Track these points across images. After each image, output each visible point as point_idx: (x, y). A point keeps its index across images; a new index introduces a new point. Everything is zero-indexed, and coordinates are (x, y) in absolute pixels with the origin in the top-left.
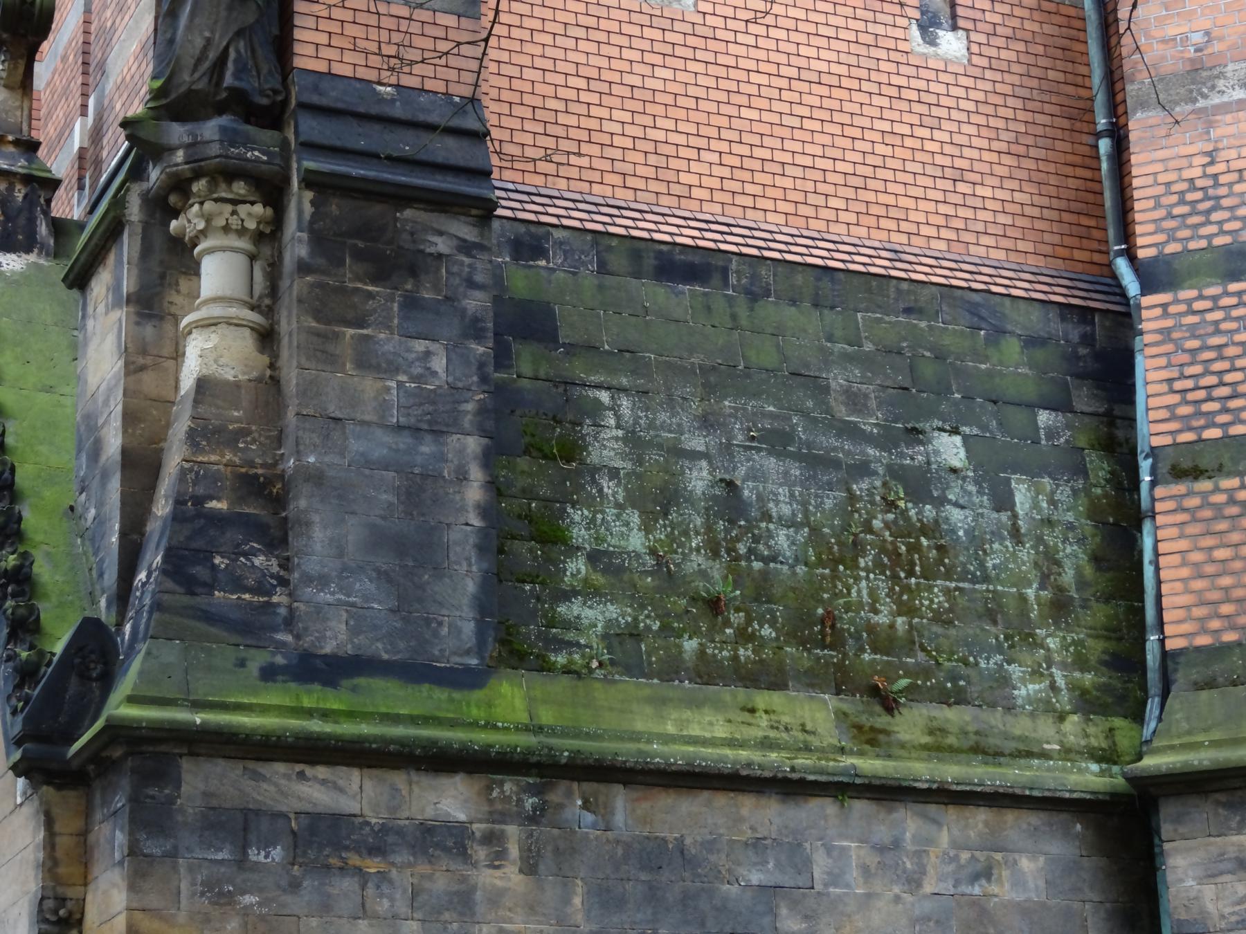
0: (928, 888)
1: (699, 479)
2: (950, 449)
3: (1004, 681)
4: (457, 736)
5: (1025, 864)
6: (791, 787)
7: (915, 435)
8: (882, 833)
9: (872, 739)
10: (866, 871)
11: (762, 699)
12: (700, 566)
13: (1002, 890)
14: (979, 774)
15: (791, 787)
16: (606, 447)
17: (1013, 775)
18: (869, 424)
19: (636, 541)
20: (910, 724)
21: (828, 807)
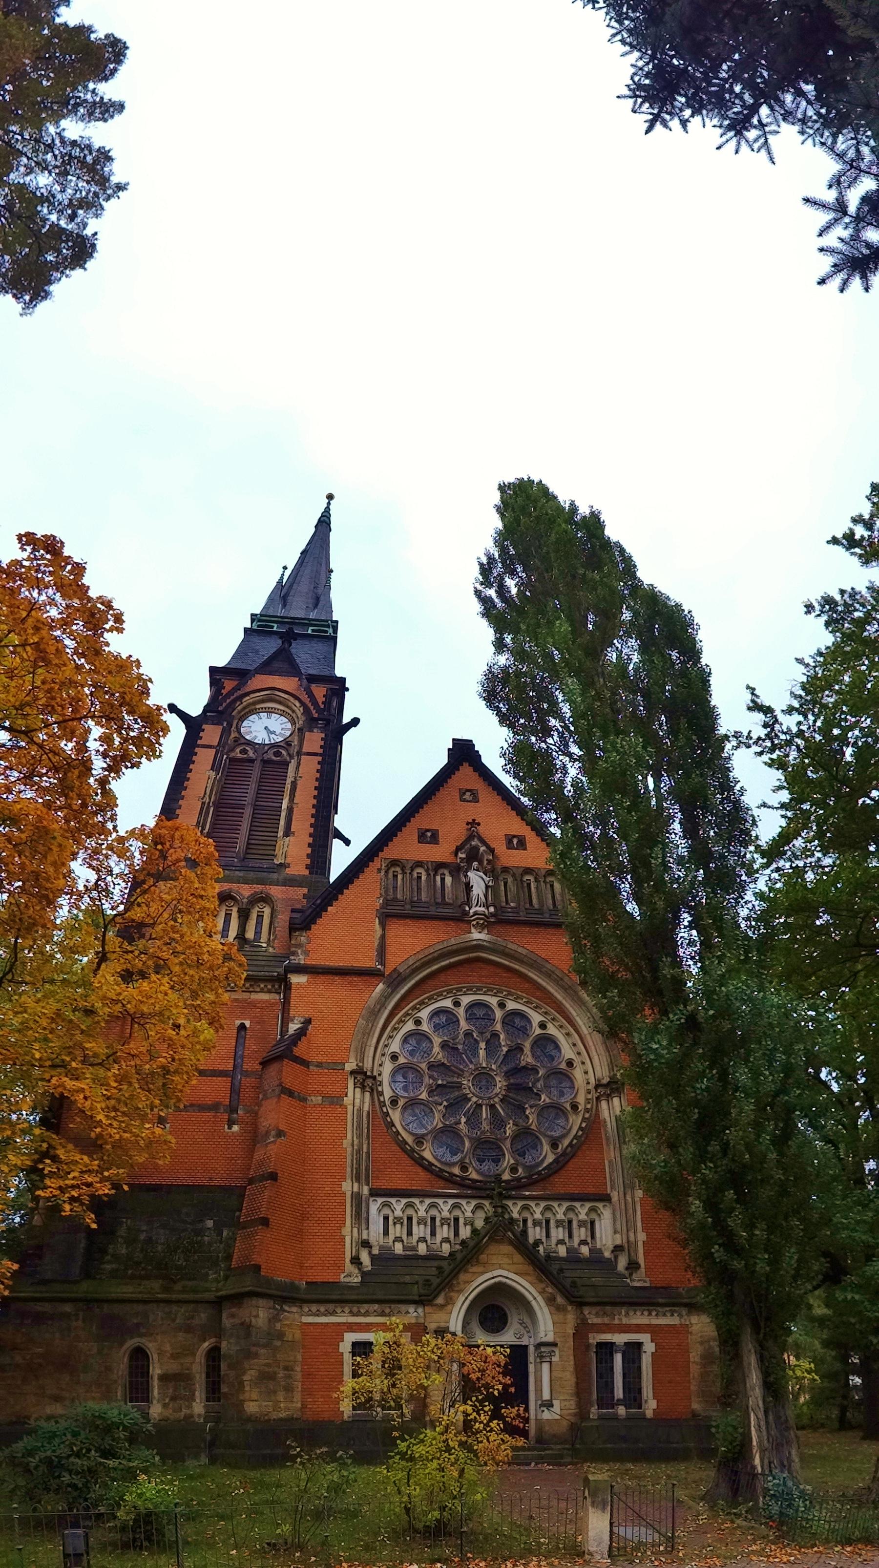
0: (178, 1321)
1: (142, 1237)
2: (210, 1223)
3: (207, 1274)
4: (73, 1295)
5: (202, 1315)
6: (145, 1302)
7: (201, 1221)
8: (167, 1310)
9: (166, 1289)
10: (162, 1319)
11: (144, 1282)
12: (138, 1256)
13: (196, 1322)
14: (191, 1296)
15: (145, 1302)
16: (122, 1231)
17: (199, 1296)
18: (189, 1220)
19: (124, 1251)
20: (178, 1287)
21: (155, 1305)
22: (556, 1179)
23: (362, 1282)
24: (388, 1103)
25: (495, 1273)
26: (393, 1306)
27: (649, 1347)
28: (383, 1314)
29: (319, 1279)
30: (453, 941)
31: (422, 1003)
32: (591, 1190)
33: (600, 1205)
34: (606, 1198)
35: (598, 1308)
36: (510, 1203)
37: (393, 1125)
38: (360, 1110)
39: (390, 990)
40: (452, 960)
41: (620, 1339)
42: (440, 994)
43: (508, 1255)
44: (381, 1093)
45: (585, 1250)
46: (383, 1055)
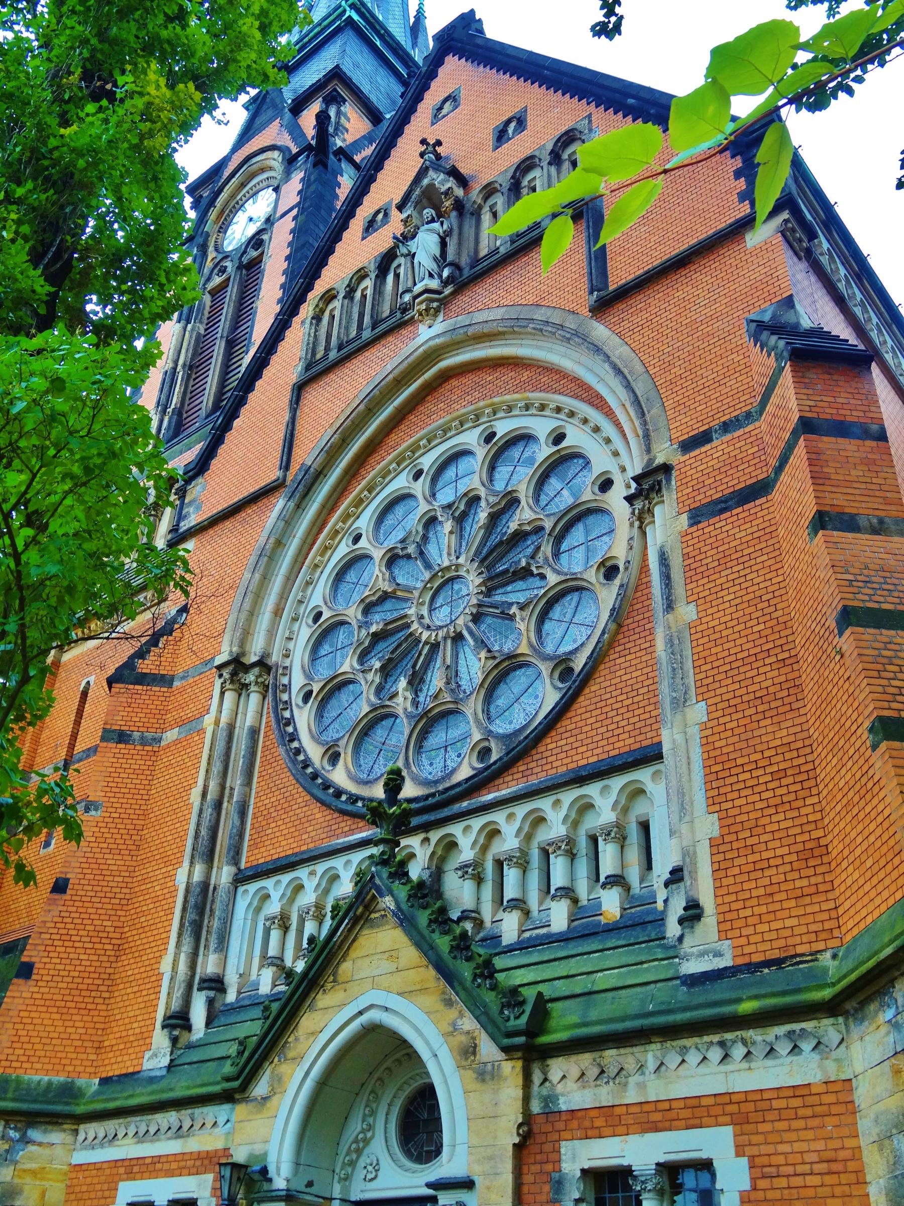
22: (549, 744)
23: (170, 1067)
24: (296, 698)
25: (362, 1003)
26: (199, 1112)
27: (733, 1177)
28: (179, 1133)
29: (116, 1071)
30: (389, 368)
31: (359, 502)
32: (625, 744)
33: (643, 775)
34: (651, 756)
35: (585, 1060)
36: (455, 829)
37: (294, 737)
38: (231, 728)
39: (291, 504)
40: (397, 402)
41: (642, 1152)
42: (385, 473)
43: (392, 954)
44: (287, 688)
45: (611, 904)
46: (295, 619)
